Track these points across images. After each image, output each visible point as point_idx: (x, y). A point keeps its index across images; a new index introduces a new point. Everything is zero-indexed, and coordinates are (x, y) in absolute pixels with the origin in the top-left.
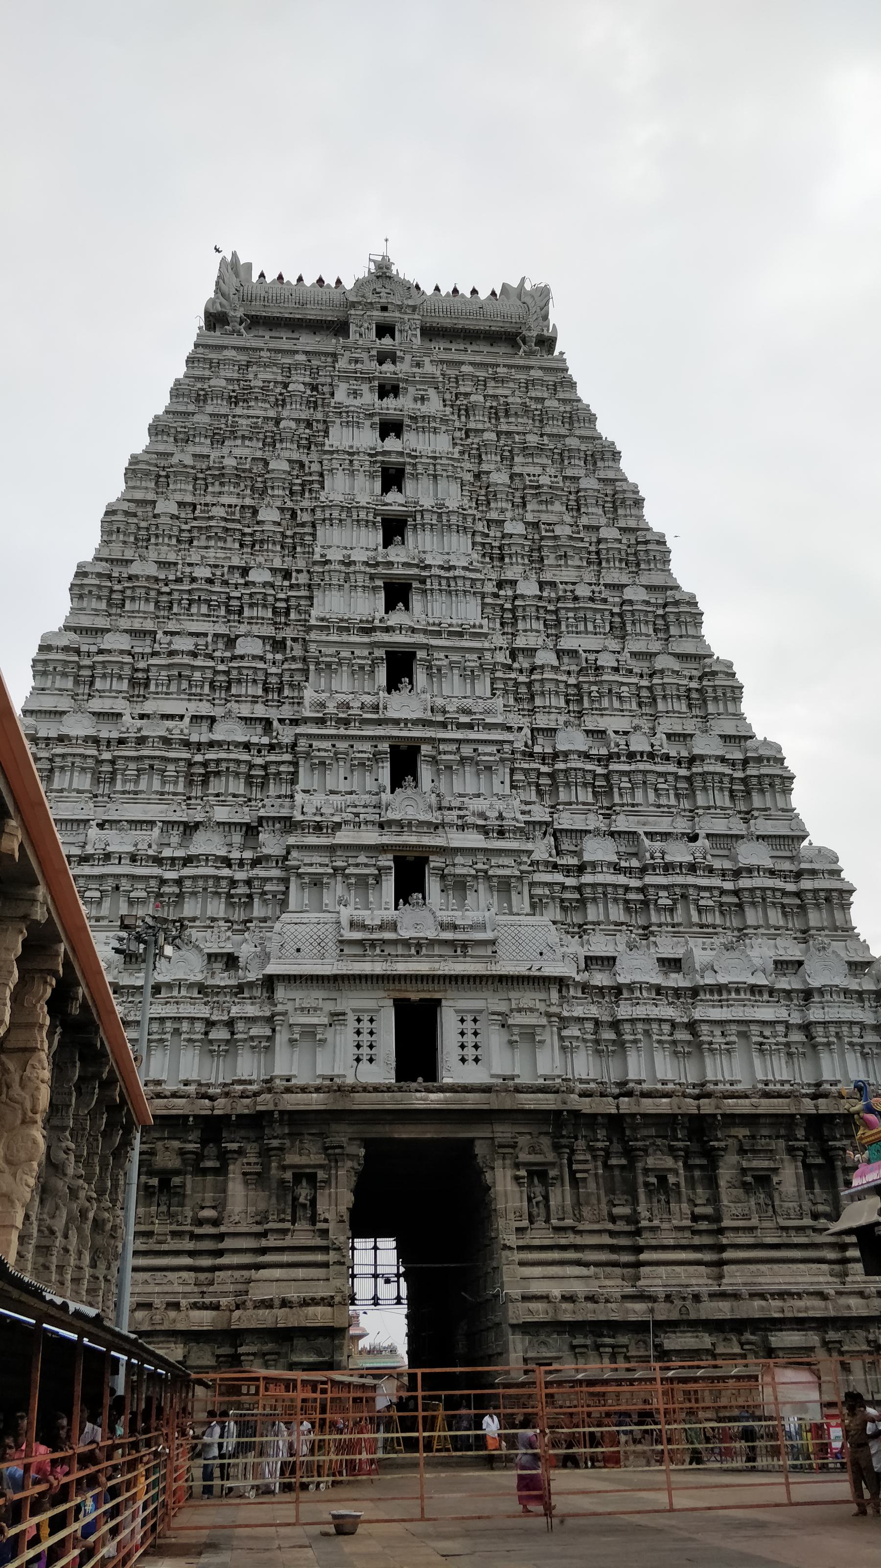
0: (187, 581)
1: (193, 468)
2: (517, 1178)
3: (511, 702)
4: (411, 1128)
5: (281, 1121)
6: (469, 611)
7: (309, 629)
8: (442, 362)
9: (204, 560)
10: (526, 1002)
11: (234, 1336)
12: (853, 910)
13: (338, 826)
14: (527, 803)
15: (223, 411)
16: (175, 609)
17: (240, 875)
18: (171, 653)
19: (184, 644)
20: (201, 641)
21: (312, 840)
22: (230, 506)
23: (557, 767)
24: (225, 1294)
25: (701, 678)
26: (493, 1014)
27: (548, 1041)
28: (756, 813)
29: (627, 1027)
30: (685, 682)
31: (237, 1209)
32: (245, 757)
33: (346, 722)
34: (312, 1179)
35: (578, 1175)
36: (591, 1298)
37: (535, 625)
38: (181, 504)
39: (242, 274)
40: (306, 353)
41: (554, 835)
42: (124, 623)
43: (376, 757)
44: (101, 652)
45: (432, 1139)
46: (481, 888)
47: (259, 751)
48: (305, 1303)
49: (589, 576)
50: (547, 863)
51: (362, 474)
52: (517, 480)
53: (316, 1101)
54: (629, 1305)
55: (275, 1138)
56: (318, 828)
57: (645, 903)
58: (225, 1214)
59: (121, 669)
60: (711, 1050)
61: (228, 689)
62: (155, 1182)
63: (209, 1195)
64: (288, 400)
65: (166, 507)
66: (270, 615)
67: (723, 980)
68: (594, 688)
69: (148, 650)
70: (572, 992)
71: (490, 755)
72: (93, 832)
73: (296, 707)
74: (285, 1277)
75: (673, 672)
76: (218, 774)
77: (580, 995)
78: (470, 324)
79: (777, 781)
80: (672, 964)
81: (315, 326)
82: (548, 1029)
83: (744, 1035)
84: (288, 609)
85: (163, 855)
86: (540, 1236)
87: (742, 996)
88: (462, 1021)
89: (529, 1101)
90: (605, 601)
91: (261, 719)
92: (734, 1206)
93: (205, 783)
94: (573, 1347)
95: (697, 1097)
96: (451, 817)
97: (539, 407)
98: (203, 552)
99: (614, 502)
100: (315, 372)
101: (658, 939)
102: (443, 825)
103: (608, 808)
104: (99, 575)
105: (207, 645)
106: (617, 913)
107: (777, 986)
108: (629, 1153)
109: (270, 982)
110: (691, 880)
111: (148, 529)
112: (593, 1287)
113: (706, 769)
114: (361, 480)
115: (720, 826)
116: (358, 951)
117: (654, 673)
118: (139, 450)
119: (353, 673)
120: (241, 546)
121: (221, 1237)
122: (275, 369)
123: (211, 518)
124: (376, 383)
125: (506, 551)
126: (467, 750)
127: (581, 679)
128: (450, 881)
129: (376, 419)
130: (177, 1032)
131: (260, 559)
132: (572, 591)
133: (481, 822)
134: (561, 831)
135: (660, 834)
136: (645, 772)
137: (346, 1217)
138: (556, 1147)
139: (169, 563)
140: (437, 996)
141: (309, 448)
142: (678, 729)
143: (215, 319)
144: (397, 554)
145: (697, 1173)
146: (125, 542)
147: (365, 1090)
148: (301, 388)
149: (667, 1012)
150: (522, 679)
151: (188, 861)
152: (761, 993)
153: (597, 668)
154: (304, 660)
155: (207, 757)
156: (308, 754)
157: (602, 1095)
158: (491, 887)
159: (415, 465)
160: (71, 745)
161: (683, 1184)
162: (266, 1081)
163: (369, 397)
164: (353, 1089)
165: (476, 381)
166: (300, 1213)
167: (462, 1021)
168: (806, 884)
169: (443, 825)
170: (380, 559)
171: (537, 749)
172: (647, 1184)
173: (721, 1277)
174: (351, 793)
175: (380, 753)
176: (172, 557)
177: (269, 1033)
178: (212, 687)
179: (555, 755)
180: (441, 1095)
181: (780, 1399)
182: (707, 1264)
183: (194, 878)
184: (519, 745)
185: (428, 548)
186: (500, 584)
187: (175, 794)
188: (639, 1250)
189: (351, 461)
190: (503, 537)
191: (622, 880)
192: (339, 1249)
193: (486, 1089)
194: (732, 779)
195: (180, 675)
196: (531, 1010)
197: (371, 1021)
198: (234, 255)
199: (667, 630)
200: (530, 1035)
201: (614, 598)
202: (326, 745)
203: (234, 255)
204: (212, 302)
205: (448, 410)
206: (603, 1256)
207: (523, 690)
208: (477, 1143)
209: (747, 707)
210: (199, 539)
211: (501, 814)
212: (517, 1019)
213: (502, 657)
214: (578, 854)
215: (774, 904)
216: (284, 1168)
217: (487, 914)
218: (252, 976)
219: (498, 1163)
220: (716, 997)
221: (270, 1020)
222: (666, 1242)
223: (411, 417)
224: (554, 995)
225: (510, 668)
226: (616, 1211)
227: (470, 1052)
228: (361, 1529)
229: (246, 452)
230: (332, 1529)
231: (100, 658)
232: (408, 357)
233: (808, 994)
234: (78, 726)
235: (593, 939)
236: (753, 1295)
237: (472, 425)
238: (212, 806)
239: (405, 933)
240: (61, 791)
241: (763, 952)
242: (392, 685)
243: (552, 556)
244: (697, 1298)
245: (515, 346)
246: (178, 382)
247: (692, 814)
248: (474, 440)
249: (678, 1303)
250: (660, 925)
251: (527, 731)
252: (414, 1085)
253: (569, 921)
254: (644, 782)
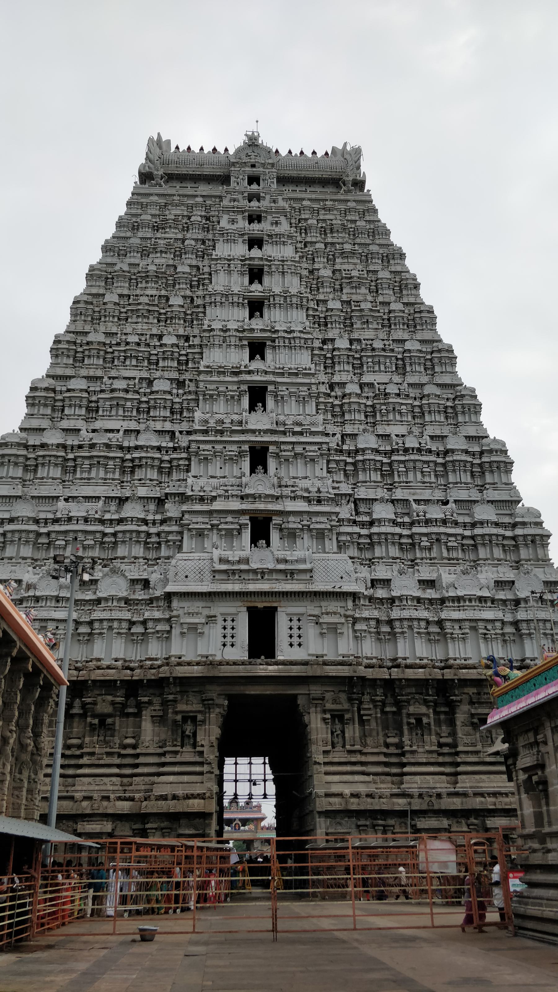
0: (123, 344)
1: (129, 272)
2: (324, 719)
3: (329, 417)
4: (257, 687)
5: (175, 683)
6: (303, 360)
7: (200, 373)
8: (290, 199)
9: (134, 331)
10: (331, 609)
11: (144, 817)
12: (550, 547)
13: (214, 498)
14: (338, 482)
15: (149, 235)
16: (116, 363)
17: (153, 530)
18: (113, 391)
19: (120, 384)
20: (131, 382)
21: (198, 507)
22: (152, 296)
23: (357, 458)
24: (138, 791)
25: (454, 399)
26: (310, 616)
27: (346, 633)
28: (487, 486)
29: (397, 624)
30: (443, 402)
31: (148, 738)
32: (158, 455)
33: (221, 432)
34: (194, 719)
35: (364, 718)
36: (370, 796)
37: (346, 368)
38: (121, 296)
39: (164, 147)
40: (203, 196)
41: (355, 502)
42: (84, 372)
43: (241, 454)
44: (69, 390)
45: (271, 695)
46: (306, 536)
47: (167, 452)
48: (188, 797)
49: (382, 335)
50: (349, 520)
51: (236, 273)
52: (337, 274)
53: (196, 671)
54: (395, 800)
55: (171, 694)
56: (202, 499)
57: (413, 545)
58: (140, 742)
59: (81, 401)
60: (452, 638)
61: (148, 412)
62: (96, 721)
63: (131, 730)
64: (190, 227)
65: (111, 297)
66: (176, 365)
67: (460, 593)
68: (383, 407)
69: (98, 389)
70: (362, 602)
71: (314, 451)
72: (61, 504)
73: (191, 423)
74: (176, 781)
75: (436, 395)
76: (140, 466)
77: (367, 603)
78: (310, 174)
79: (502, 465)
80: (430, 584)
81: (209, 179)
82: (346, 625)
83: (474, 629)
84: (187, 361)
85: (105, 518)
86: (338, 756)
87: (473, 604)
88: (291, 620)
89: (332, 671)
90: (392, 350)
91: (169, 431)
92: (465, 738)
93: (132, 472)
94: (358, 826)
95: (442, 668)
96: (287, 491)
97: (353, 226)
98: (134, 326)
99: (400, 286)
100: (208, 208)
101: (420, 568)
102: (282, 497)
103: (391, 485)
104: (68, 342)
105: (135, 385)
106: (394, 551)
107: (496, 597)
108: (397, 703)
109: (169, 596)
110: (442, 530)
111: (99, 312)
112: (372, 788)
113: (455, 458)
114: (235, 277)
115: (463, 495)
116: (224, 577)
117: (424, 396)
118: (94, 262)
119: (227, 400)
120: (159, 321)
121: (137, 756)
122: (183, 208)
123: (139, 304)
124: (247, 214)
125: (329, 320)
126: (299, 449)
127: (375, 402)
128: (285, 532)
129: (246, 237)
130: (110, 628)
131: (170, 329)
132: (371, 345)
133: (306, 495)
134: (360, 499)
135: (424, 500)
136: (415, 461)
137: (215, 744)
138: (350, 700)
139: (113, 334)
140: (275, 605)
141: (203, 258)
142: (438, 433)
143: (145, 177)
144: (257, 324)
145: (442, 717)
146: (85, 321)
147: (228, 664)
148: (199, 219)
149: (424, 614)
150: (337, 402)
151: (120, 521)
152: (486, 602)
153: (386, 394)
154: (196, 393)
155: (134, 456)
156: (197, 453)
157: (380, 667)
158: (312, 536)
159: (270, 266)
160: (48, 450)
161: (432, 723)
162: (166, 659)
163: (242, 224)
164: (220, 663)
165: (313, 211)
166: (186, 741)
167: (291, 620)
168: (519, 531)
169: (282, 497)
170: (246, 327)
171: (345, 447)
172: (409, 724)
173: (456, 783)
174: (224, 477)
175: (243, 451)
176: (114, 330)
177: (168, 628)
178: (138, 411)
179: (357, 451)
180: (276, 667)
181: (429, 860)
182: (447, 774)
183: (124, 532)
184: (333, 445)
185: (277, 320)
186: (324, 342)
187: (113, 479)
188: (404, 765)
189: (229, 265)
190: (327, 311)
191: (398, 530)
192: (210, 763)
193: (305, 663)
194: (472, 464)
195: (118, 404)
196: (335, 613)
197: (233, 620)
198: (159, 134)
199: (433, 368)
200: (334, 629)
201: (398, 349)
202: (209, 447)
203: (159, 134)
204: (143, 166)
205: (293, 229)
206: (379, 769)
207: (337, 409)
208: (299, 697)
209: (484, 418)
210: (132, 318)
211: (319, 489)
212: (325, 619)
213: (323, 389)
214: (370, 514)
215: (497, 544)
216: (176, 713)
217: (307, 553)
218: (158, 593)
219: (313, 710)
220: (456, 604)
221: (169, 620)
222: (420, 760)
223: (268, 235)
224: (350, 604)
225: (329, 395)
226: (389, 740)
227: (295, 640)
228: (157, 938)
229: (163, 261)
230: (138, 937)
231: (68, 395)
232: (268, 197)
233: (517, 602)
234: (53, 438)
235: (378, 568)
236: (476, 794)
237: (309, 239)
238: (136, 487)
239: (254, 566)
240: (42, 478)
241: (487, 575)
242: (252, 408)
243: (359, 322)
244: (439, 796)
245: (338, 187)
246: (121, 218)
247: (446, 487)
248: (310, 248)
249: (427, 799)
250: (422, 559)
251: (339, 436)
252: (259, 661)
253: (363, 557)
254: (414, 468)
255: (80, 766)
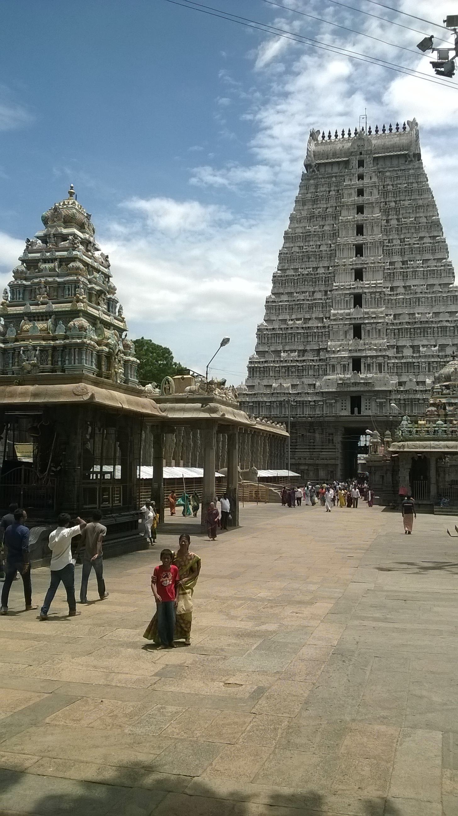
50: (393, 357)
124: (356, 190)
147: (343, 416)
171: (395, 322)
202: (337, 327)
218: (318, 391)
224: (388, 394)
239: (352, 381)
251: (392, 316)
255: (297, 449)
